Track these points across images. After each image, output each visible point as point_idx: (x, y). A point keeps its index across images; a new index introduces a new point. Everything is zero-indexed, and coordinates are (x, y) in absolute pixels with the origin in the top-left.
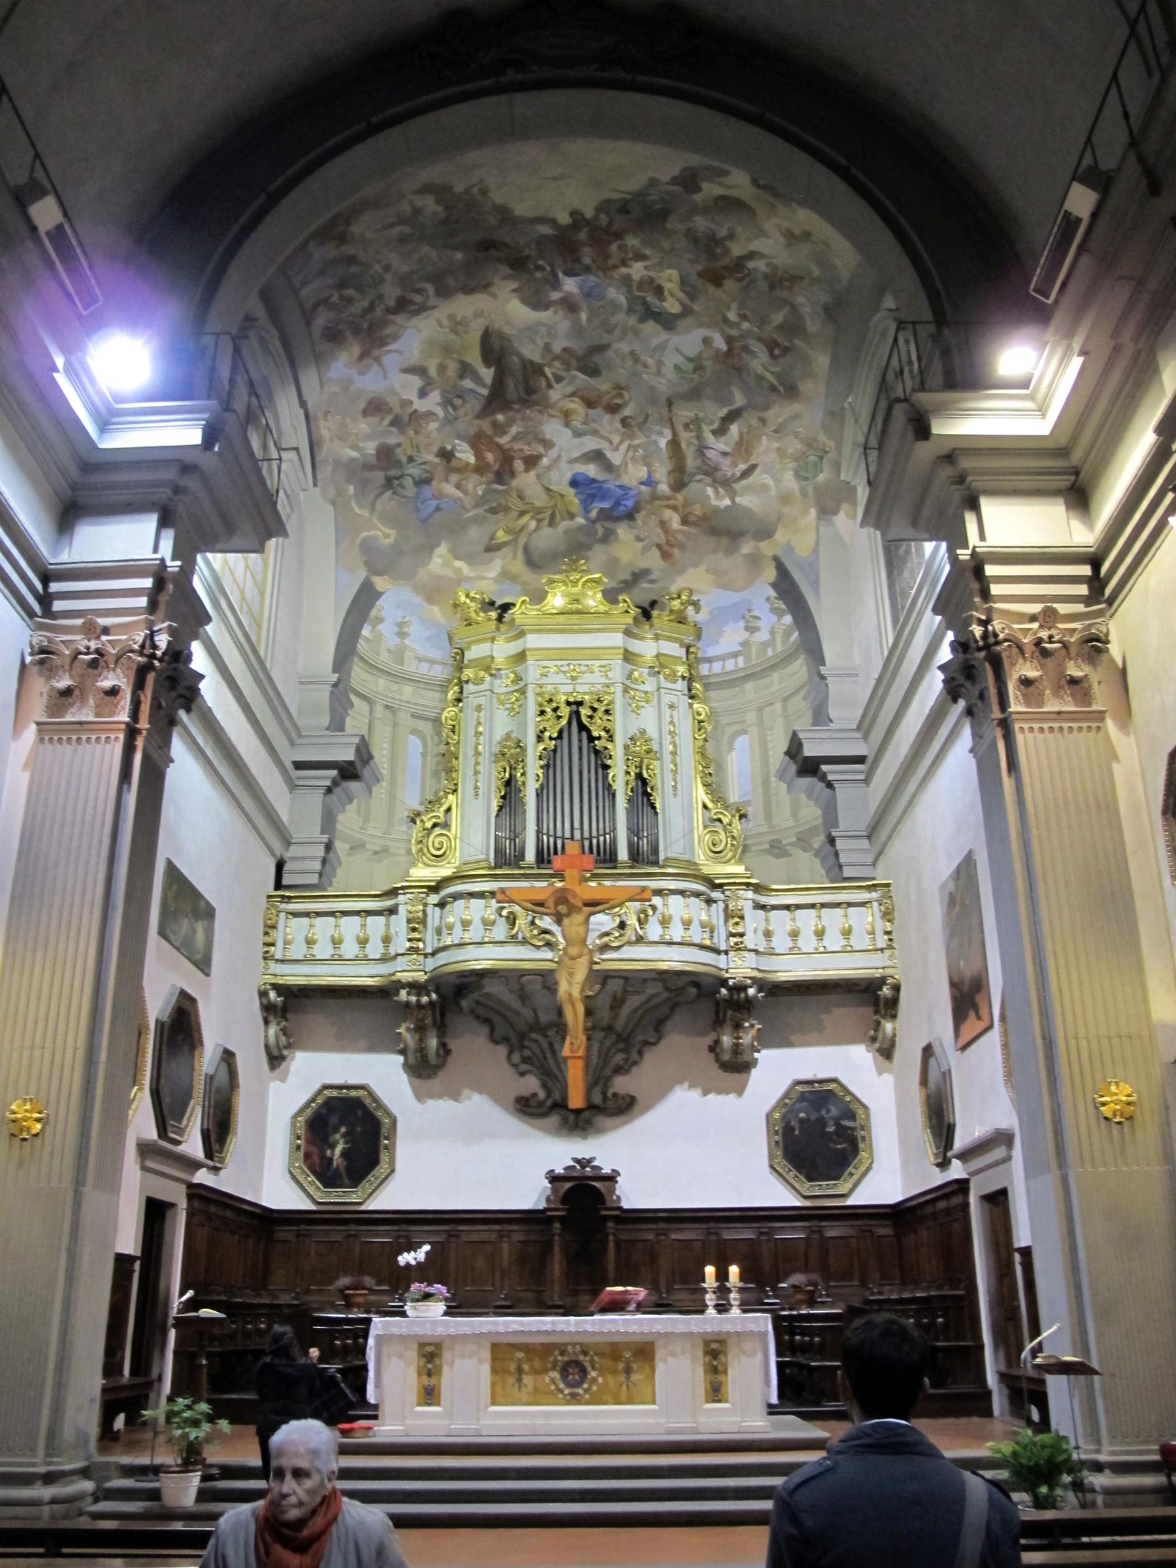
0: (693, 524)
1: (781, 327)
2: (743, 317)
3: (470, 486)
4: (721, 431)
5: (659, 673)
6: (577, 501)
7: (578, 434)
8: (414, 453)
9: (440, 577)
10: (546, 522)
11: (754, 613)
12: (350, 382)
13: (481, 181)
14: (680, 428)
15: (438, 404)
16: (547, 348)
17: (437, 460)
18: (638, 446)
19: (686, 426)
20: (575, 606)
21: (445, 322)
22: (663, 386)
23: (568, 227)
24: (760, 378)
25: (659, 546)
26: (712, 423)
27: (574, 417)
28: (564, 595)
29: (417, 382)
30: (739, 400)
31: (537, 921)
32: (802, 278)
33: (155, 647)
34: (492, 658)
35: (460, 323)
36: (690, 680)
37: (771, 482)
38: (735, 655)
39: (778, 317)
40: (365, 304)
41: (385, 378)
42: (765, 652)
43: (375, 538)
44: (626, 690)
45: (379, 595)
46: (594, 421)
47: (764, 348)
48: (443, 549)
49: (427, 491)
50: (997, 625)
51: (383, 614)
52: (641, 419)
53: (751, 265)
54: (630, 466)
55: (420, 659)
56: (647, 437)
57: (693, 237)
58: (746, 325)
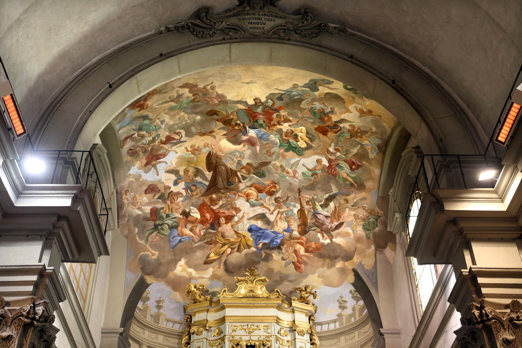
0: (311, 252)
1: (355, 155)
2: (337, 150)
3: (197, 230)
4: (325, 206)
6: (252, 239)
7: (253, 205)
8: (170, 213)
9: (180, 277)
10: (236, 249)
11: (343, 299)
12: (140, 176)
13: (212, 83)
14: (304, 204)
15: (183, 189)
16: (239, 163)
17: (181, 217)
18: (283, 212)
19: (308, 203)
20: (251, 294)
21: (189, 149)
22: (296, 183)
23: (252, 106)
24: (345, 180)
25: (294, 263)
26: (321, 201)
27: (251, 197)
28: (245, 288)
29: (173, 177)
30: (335, 190)
32: (367, 132)
33: (35, 314)
34: (207, 321)
35: (196, 150)
36: (311, 334)
37: (350, 231)
38: (334, 321)
39: (355, 151)
40: (151, 139)
41: (158, 175)
42: (350, 321)
43: (147, 256)
44: (277, 339)
45: (148, 285)
46: (261, 199)
47: (348, 166)
48: (182, 262)
49: (175, 232)
50: (488, 309)
51: (149, 295)
52: (285, 199)
53: (342, 125)
54: (279, 222)
55: (168, 321)
56: (287, 207)
57: (312, 111)
58: (338, 154)
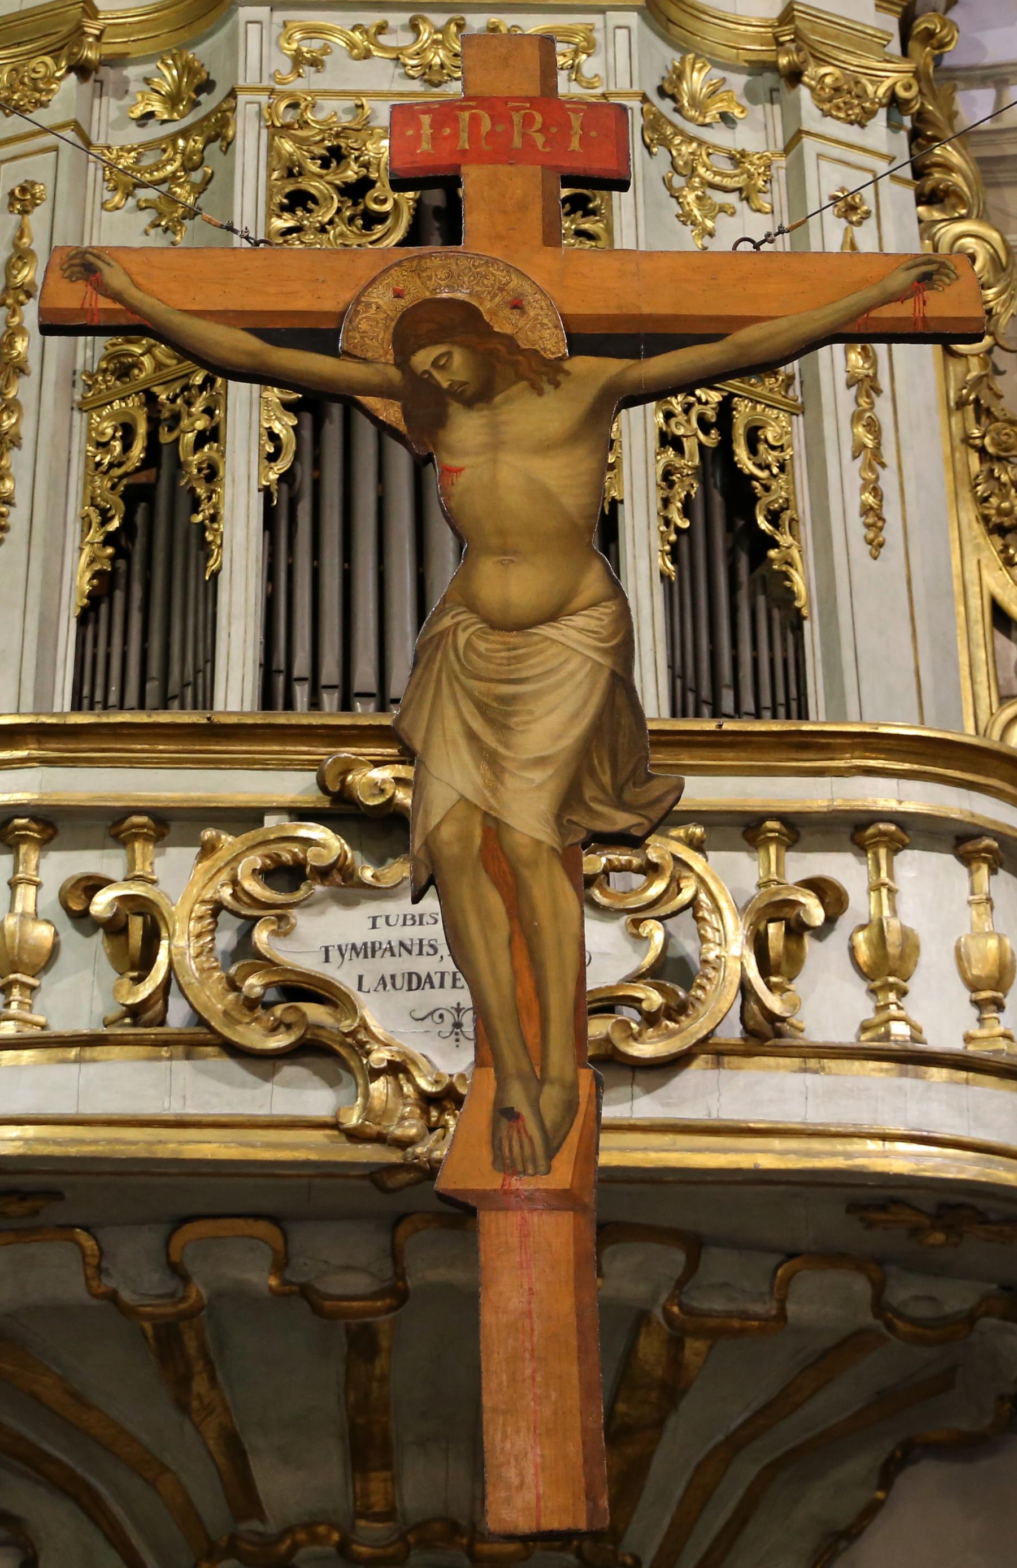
5: (794, 76)
31: (261, 936)
